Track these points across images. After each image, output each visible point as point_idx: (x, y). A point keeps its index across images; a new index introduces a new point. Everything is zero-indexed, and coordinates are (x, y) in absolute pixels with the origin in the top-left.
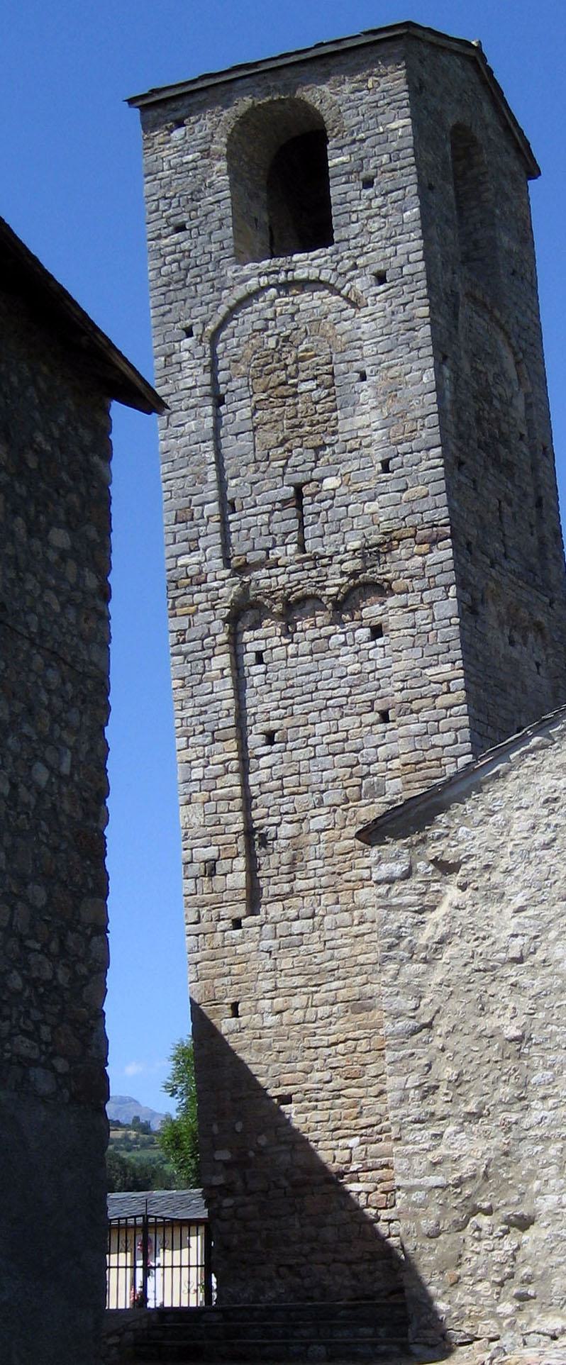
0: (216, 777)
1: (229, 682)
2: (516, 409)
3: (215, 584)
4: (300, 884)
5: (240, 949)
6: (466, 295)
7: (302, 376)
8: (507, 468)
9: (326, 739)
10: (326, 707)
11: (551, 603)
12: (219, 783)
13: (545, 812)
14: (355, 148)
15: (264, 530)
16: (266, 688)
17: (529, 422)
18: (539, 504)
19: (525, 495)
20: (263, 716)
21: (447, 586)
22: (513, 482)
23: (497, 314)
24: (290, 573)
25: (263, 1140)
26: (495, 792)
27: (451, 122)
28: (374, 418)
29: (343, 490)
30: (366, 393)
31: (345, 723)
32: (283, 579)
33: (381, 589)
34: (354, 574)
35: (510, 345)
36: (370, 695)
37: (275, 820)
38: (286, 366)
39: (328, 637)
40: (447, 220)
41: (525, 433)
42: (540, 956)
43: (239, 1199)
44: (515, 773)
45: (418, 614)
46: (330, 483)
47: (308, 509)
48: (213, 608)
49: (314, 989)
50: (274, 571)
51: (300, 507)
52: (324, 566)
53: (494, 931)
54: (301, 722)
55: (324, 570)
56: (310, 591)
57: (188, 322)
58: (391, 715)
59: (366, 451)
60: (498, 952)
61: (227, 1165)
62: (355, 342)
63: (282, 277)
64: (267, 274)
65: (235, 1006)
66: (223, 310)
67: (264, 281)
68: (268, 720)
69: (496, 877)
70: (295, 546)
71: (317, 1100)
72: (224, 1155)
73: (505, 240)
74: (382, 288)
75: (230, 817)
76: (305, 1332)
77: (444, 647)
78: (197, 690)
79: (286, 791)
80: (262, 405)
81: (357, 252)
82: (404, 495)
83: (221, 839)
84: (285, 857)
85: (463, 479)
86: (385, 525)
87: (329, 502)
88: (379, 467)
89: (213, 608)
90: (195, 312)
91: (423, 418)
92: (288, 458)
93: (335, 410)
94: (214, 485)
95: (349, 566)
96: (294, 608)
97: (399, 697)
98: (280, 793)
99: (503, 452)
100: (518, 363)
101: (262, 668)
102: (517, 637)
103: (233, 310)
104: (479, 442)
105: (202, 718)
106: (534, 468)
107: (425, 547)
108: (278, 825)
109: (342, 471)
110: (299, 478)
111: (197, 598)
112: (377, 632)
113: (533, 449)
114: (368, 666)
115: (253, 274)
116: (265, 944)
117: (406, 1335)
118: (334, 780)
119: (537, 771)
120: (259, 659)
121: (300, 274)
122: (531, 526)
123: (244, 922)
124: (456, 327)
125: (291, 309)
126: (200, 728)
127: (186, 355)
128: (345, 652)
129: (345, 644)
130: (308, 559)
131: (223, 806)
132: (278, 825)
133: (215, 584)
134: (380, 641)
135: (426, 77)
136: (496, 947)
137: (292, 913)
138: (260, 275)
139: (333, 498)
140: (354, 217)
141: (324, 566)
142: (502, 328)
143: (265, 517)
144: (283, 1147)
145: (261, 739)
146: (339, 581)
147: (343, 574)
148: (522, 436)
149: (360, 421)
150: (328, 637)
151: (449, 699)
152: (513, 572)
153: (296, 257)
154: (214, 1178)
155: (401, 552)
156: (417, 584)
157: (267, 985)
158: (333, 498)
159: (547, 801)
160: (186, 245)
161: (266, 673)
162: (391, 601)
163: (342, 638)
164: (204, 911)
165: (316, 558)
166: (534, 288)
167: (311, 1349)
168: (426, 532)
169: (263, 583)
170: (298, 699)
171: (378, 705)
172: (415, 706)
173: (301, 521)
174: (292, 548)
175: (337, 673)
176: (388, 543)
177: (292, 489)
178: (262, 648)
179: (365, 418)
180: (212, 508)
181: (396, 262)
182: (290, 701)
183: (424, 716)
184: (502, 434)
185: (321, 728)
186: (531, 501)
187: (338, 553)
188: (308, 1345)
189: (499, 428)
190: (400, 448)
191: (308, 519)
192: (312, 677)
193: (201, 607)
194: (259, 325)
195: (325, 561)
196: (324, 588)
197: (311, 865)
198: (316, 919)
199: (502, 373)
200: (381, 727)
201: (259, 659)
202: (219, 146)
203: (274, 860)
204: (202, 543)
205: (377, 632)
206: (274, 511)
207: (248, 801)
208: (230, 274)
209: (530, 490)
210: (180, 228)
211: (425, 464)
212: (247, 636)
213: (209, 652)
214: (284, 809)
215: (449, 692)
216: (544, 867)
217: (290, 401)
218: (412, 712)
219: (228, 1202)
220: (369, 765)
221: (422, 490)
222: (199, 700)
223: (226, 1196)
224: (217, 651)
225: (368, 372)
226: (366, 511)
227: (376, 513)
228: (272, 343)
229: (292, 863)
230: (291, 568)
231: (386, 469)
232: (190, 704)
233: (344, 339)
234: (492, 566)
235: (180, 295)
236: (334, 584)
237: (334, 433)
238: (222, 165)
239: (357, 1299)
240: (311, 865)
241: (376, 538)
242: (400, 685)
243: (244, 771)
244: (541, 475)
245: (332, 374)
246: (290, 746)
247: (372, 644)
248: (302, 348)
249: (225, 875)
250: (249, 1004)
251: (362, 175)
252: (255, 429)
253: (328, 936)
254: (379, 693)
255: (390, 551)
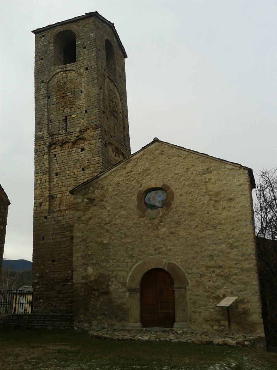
0: (43, 183)
1: (48, 161)
2: (119, 106)
3: (46, 139)
4: (62, 208)
5: (46, 224)
6: (108, 77)
7: (68, 92)
8: (117, 118)
9: (69, 175)
10: (70, 167)
11: (126, 149)
12: (44, 184)
13: (116, 186)
14: (82, 40)
15: (58, 127)
16: (56, 163)
17: (122, 109)
18: (124, 128)
19: (121, 125)
20: (56, 169)
21: (99, 139)
22: (118, 121)
23: (115, 83)
24: (63, 136)
25: (47, 271)
26: (104, 181)
27: (106, 38)
28: (84, 101)
29: (76, 118)
30: (83, 95)
31: (74, 171)
32: (61, 138)
33: (85, 139)
34: (78, 137)
35: (119, 92)
36: (81, 164)
37: (57, 193)
38: (64, 89)
39: (71, 151)
40: (103, 58)
41: (121, 111)
42: (113, 222)
43: (40, 286)
44: (109, 177)
45: (92, 145)
46: (73, 116)
47: (68, 122)
48: (45, 144)
49: (63, 233)
50: (59, 136)
51: (66, 121)
52: (71, 135)
53: (102, 216)
54: (64, 170)
55: (71, 136)
56: (67, 140)
57: (43, 80)
58: (85, 169)
59: (82, 109)
60: (103, 221)
61: (38, 277)
62: (80, 84)
63: (64, 69)
64: (61, 69)
65: (44, 237)
66: (51, 77)
67: (60, 70)
68: (56, 170)
69: (103, 203)
70: (64, 130)
71: (61, 261)
72: (38, 275)
73: (118, 69)
74: (87, 71)
75: (46, 192)
76: (48, 322)
77: (98, 153)
78: (40, 163)
79: (59, 187)
80: (58, 98)
81: (81, 63)
82: (90, 118)
83: (43, 198)
84: (58, 202)
85: (104, 116)
86: (85, 126)
87: (73, 120)
88: (84, 112)
89: (45, 144)
90: (44, 78)
91: (95, 101)
92: (64, 110)
93: (75, 99)
94: (47, 116)
95: (77, 135)
96: (63, 144)
97: (87, 164)
98: (58, 187)
99: (116, 114)
100: (120, 96)
101: (56, 158)
102: (117, 155)
103: (53, 77)
104: (109, 110)
105: (41, 169)
106: (123, 120)
107: (94, 130)
108: (57, 194)
109: (76, 113)
110: (66, 115)
111: (42, 142)
112: (83, 150)
113: (123, 115)
114: (80, 158)
115: (57, 69)
116: (52, 223)
117: (73, 324)
118: (71, 184)
119: (114, 176)
120: (55, 156)
121: (68, 69)
122: (122, 132)
123: (47, 217)
124: (104, 82)
125: (66, 76)
126: (40, 172)
127: (42, 87)
128: (76, 153)
129: (75, 152)
130: (67, 133)
131: (44, 190)
132: (57, 194)
133: (46, 139)
134: (83, 152)
135: (100, 26)
136: (103, 220)
137: (59, 215)
138: (59, 69)
139: (74, 119)
140: (81, 55)
141: (71, 135)
142: (116, 87)
143: (58, 124)
144: (52, 273)
145: (54, 175)
146: (74, 138)
147: (75, 136)
148: (120, 112)
149: (81, 102)
150: (71, 151)
151: (98, 165)
152: (116, 140)
153: (68, 65)
154: (35, 281)
155: (88, 131)
156: (92, 139)
157: (51, 232)
158: (74, 119)
159: (117, 184)
160: (43, 63)
161: (56, 159)
162: (86, 143)
163: (74, 151)
164: (38, 214)
165: (69, 133)
166: (125, 81)
167: (48, 327)
168: (95, 127)
169: (57, 139)
170: (63, 165)
171: (82, 167)
172: (90, 166)
173: (66, 125)
174: (64, 131)
175: (73, 159)
176: (86, 129)
177: (65, 117)
178: (56, 153)
179: (82, 101)
180: (46, 122)
181: (90, 65)
182: (62, 166)
183: (92, 169)
184: (115, 110)
185: (68, 172)
186: (122, 127)
187: (74, 132)
188: (47, 326)
189: (115, 109)
190: (89, 108)
191: (68, 124)
192: (67, 160)
193: (42, 144)
194: (59, 80)
195: (71, 133)
196: (71, 140)
197: (64, 204)
198: (64, 217)
199: (116, 97)
200: (82, 172)
201: (55, 156)
202: (52, 40)
203: (56, 203)
204: (43, 130)
205: (83, 150)
206: (60, 122)
207: (50, 189)
208: (53, 69)
209: (122, 124)
210: (42, 59)
211: (95, 111)
212: (53, 151)
213: (43, 154)
214: (59, 191)
215: (98, 163)
216: (115, 200)
217: (65, 97)
218: (89, 168)
219: (38, 287)
220: (79, 180)
221: (94, 117)
222: (41, 165)
223: (37, 285)
224: (45, 154)
225: (83, 90)
226: (81, 122)
227: (82, 123)
228: (61, 84)
229: (60, 204)
230: (63, 135)
231: (86, 112)
232: (38, 166)
233: (78, 83)
234: (111, 137)
235: (41, 74)
236: (73, 138)
237: (75, 105)
238: (52, 45)
239: (67, 313)
240: (64, 204)
241: (83, 128)
242: (87, 162)
243: (50, 181)
244: (125, 122)
245: (75, 91)
246: (61, 176)
247: (81, 153)
248: (68, 85)
249: (44, 206)
250: (47, 237)
251: (83, 46)
252: (57, 104)
253: (67, 220)
254: (82, 164)
255: (86, 131)
